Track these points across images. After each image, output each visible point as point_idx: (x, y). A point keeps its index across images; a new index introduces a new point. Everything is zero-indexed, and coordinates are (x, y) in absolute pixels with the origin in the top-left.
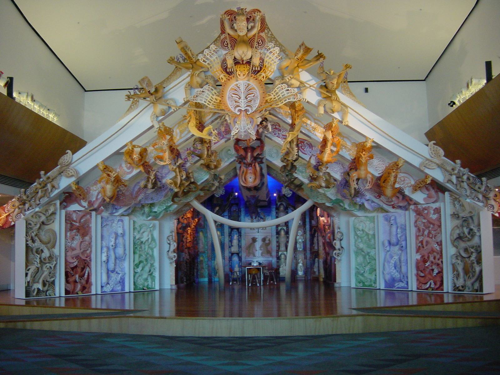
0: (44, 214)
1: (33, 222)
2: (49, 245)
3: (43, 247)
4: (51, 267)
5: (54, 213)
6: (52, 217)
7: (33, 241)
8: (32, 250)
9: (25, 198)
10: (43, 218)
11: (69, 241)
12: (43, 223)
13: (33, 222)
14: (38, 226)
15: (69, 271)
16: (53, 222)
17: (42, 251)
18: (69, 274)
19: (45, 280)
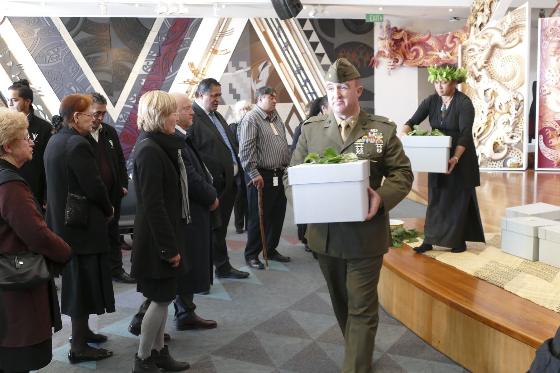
0: (500, 31)
1: (478, 45)
2: (512, 84)
3: (493, 85)
4: (508, 122)
5: (514, 28)
6: (515, 34)
7: (477, 79)
8: (477, 93)
9: (477, 7)
10: (497, 38)
11: (553, 73)
12: (495, 47)
13: (478, 45)
14: (487, 51)
15: (552, 126)
16: (520, 41)
17: (494, 94)
18: (550, 132)
19: (499, 141)
